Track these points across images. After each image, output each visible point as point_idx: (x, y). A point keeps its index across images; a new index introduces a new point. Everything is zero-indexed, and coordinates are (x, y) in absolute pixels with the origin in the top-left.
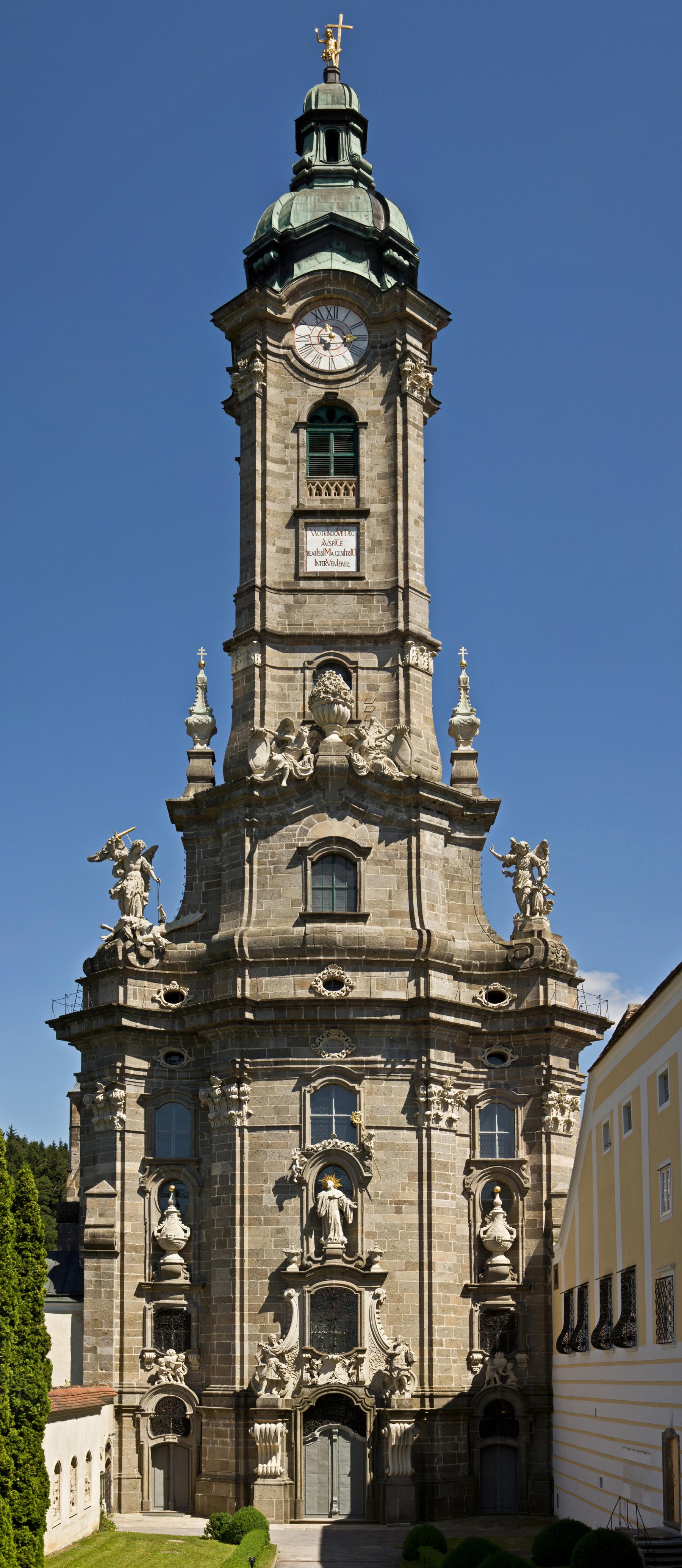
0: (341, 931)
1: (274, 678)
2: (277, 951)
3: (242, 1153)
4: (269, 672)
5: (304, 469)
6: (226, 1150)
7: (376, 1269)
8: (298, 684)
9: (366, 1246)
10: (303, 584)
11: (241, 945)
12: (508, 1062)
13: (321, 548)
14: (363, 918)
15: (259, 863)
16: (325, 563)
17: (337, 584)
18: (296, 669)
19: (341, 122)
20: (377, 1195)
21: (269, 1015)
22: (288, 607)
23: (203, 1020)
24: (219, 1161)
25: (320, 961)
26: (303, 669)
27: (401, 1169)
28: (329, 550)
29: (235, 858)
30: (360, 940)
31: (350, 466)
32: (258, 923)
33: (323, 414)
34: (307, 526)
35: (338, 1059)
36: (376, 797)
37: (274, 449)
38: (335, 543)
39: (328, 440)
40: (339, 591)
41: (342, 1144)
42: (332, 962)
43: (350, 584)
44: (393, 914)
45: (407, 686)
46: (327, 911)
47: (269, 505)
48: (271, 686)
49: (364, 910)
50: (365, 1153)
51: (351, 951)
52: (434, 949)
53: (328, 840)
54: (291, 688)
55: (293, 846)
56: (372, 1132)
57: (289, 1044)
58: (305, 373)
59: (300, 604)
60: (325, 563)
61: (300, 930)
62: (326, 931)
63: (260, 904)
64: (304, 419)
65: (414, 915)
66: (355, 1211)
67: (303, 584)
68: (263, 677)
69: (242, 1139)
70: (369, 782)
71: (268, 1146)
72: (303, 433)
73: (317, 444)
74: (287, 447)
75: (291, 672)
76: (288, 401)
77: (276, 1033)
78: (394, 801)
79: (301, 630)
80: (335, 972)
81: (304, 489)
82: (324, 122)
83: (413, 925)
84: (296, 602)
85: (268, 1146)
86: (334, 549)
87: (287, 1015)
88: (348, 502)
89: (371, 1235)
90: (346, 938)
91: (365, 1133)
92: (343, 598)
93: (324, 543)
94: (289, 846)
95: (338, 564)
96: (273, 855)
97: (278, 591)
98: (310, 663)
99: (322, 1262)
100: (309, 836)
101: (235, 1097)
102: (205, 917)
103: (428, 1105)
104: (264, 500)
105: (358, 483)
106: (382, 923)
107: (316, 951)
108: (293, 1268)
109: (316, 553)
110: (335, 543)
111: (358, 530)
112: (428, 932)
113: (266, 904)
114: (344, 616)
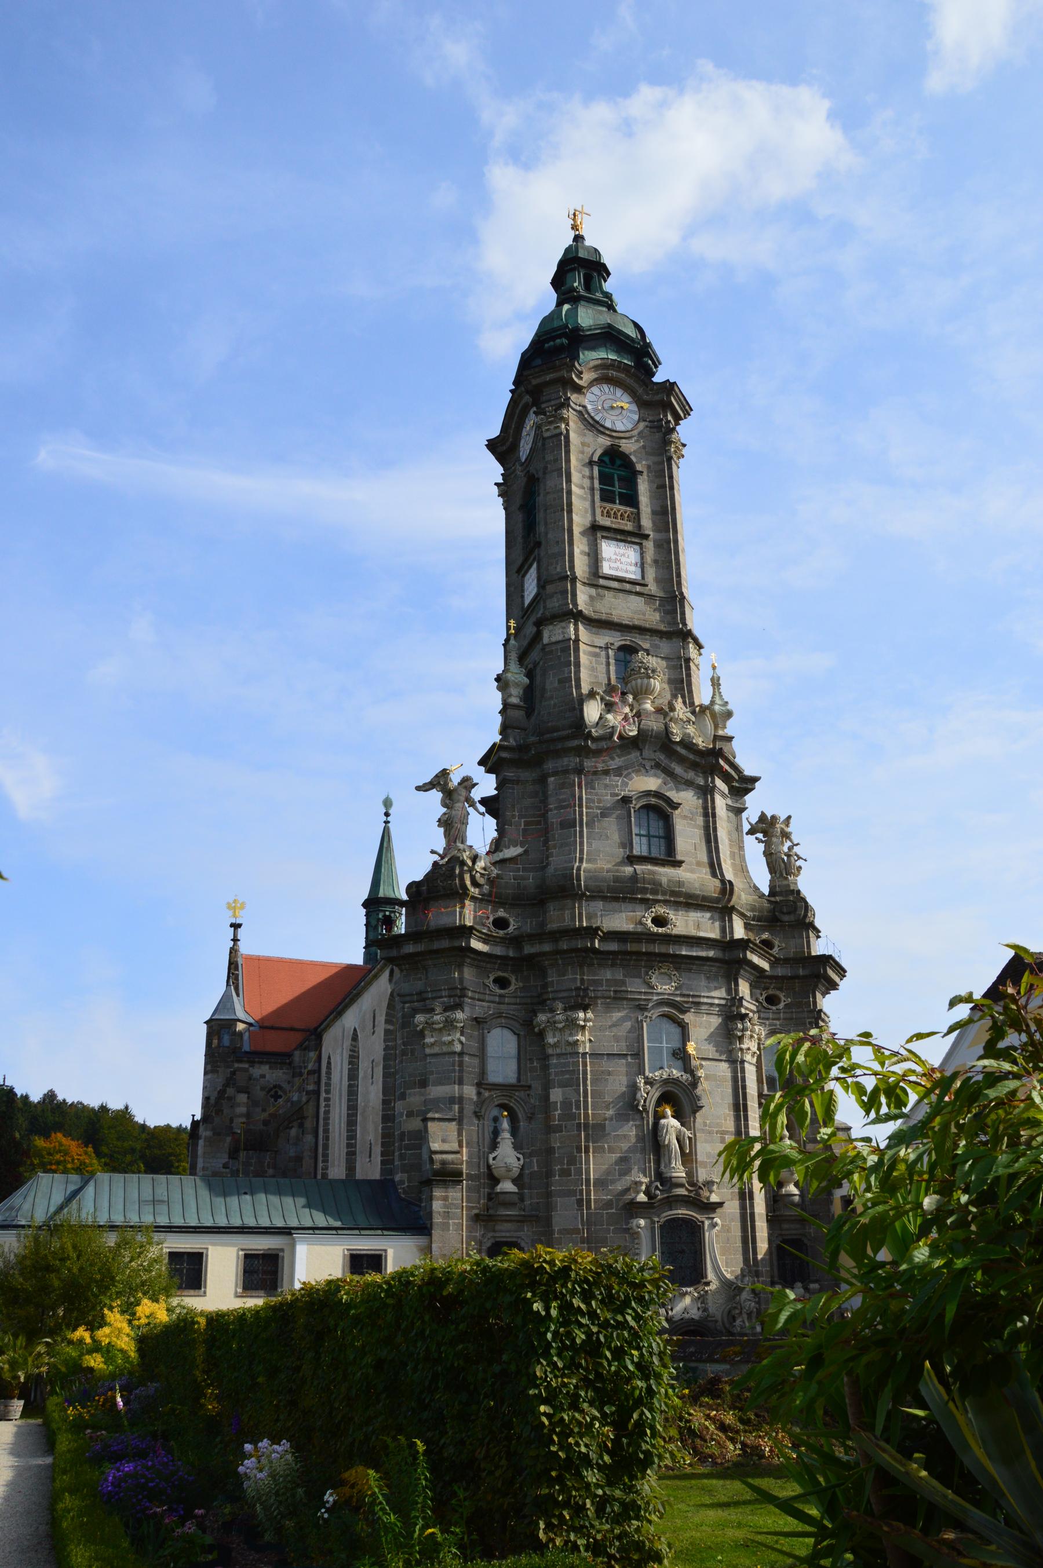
0: (665, 874)
1: (584, 653)
2: (610, 889)
3: (585, 1079)
4: (582, 646)
5: (597, 497)
6: (567, 1076)
7: (714, 1198)
8: (604, 660)
9: (702, 1175)
10: (602, 582)
11: (579, 879)
12: (781, 1005)
13: (614, 557)
14: (678, 864)
15: (587, 808)
16: (617, 569)
17: (628, 586)
18: (601, 647)
19: (595, 270)
20: (705, 1124)
21: (613, 946)
22: (591, 597)
23: (547, 947)
24: (559, 1087)
25: (649, 899)
26: (607, 648)
27: (722, 1100)
28: (620, 559)
29: (564, 800)
30: (680, 883)
31: (631, 500)
32: (589, 861)
33: (606, 459)
34: (603, 537)
35: (668, 991)
36: (681, 760)
37: (575, 477)
38: (624, 555)
39: (613, 478)
40: (630, 592)
41: (676, 1073)
42: (658, 901)
43: (638, 588)
44: (699, 864)
45: (689, 675)
46: (645, 853)
47: (575, 517)
48: (584, 659)
49: (679, 858)
50: (695, 1082)
51: (673, 893)
52: (734, 898)
53: (648, 793)
54: (597, 662)
55: (617, 795)
56: (704, 1063)
57: (625, 976)
58: (594, 426)
59: (601, 597)
60: (617, 569)
61: (628, 870)
62: (653, 873)
63: (589, 844)
64: (596, 458)
65: (715, 867)
66: (690, 1138)
67: (602, 582)
68: (577, 650)
69: (585, 1065)
70: (678, 749)
71: (609, 1073)
72: (596, 469)
73: (604, 479)
74: (584, 477)
75: (597, 650)
76: (583, 444)
77: (612, 965)
78: (694, 766)
79: (604, 617)
80: (661, 910)
81: (598, 511)
82: (583, 267)
83: (714, 875)
84: (598, 594)
85: (609, 1073)
86: (623, 559)
87: (630, 947)
88: (629, 526)
89: (704, 1165)
90: (669, 881)
91: (695, 1063)
92: (633, 598)
93: (615, 554)
94: (614, 795)
95: (627, 571)
96: (599, 801)
97: (584, 584)
98: (612, 644)
99: (669, 1191)
100: (630, 787)
101: (582, 1023)
102: (526, 852)
103: (741, 1039)
104: (570, 512)
105: (638, 514)
106: (692, 871)
107: (644, 890)
108: (642, 1197)
109: (610, 560)
110: (624, 555)
111: (641, 549)
112: (730, 882)
113: (595, 844)
114: (635, 613)
